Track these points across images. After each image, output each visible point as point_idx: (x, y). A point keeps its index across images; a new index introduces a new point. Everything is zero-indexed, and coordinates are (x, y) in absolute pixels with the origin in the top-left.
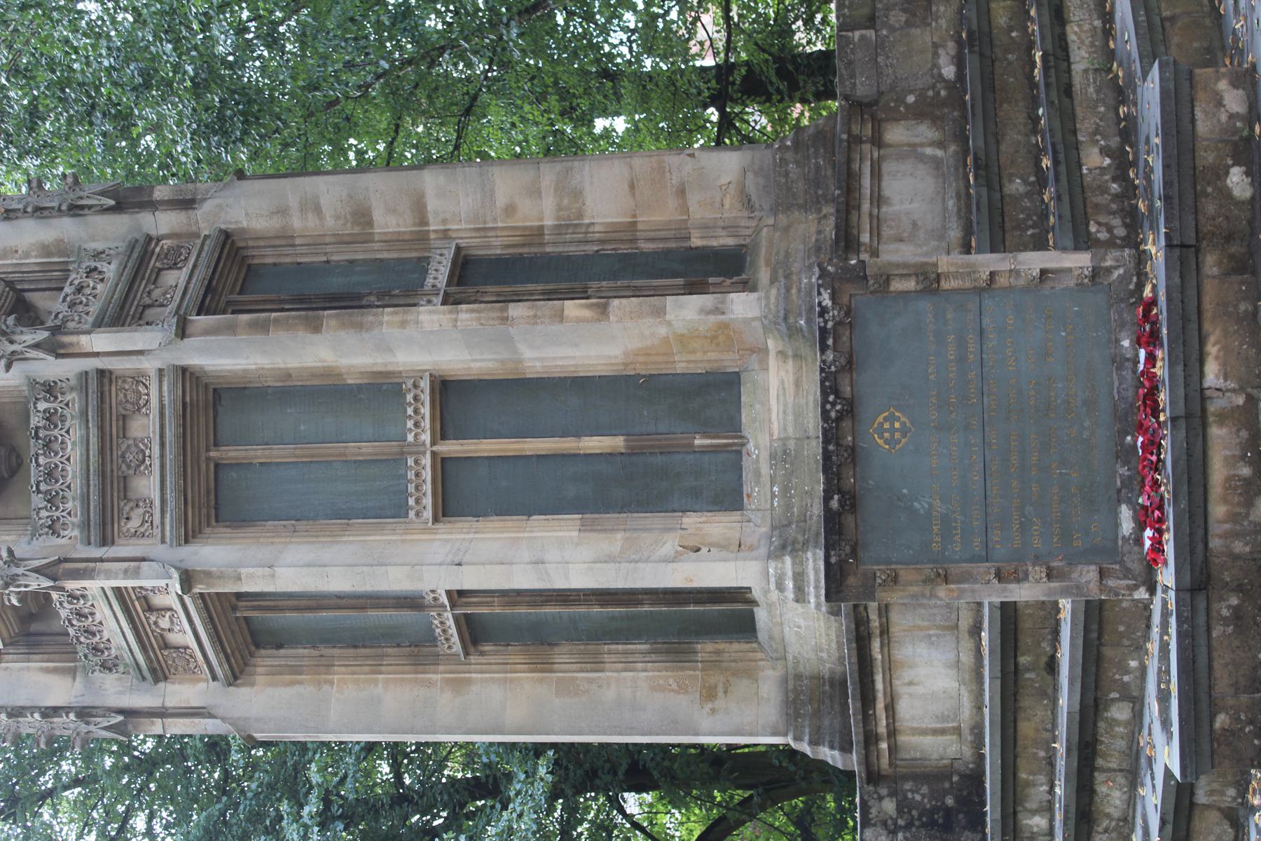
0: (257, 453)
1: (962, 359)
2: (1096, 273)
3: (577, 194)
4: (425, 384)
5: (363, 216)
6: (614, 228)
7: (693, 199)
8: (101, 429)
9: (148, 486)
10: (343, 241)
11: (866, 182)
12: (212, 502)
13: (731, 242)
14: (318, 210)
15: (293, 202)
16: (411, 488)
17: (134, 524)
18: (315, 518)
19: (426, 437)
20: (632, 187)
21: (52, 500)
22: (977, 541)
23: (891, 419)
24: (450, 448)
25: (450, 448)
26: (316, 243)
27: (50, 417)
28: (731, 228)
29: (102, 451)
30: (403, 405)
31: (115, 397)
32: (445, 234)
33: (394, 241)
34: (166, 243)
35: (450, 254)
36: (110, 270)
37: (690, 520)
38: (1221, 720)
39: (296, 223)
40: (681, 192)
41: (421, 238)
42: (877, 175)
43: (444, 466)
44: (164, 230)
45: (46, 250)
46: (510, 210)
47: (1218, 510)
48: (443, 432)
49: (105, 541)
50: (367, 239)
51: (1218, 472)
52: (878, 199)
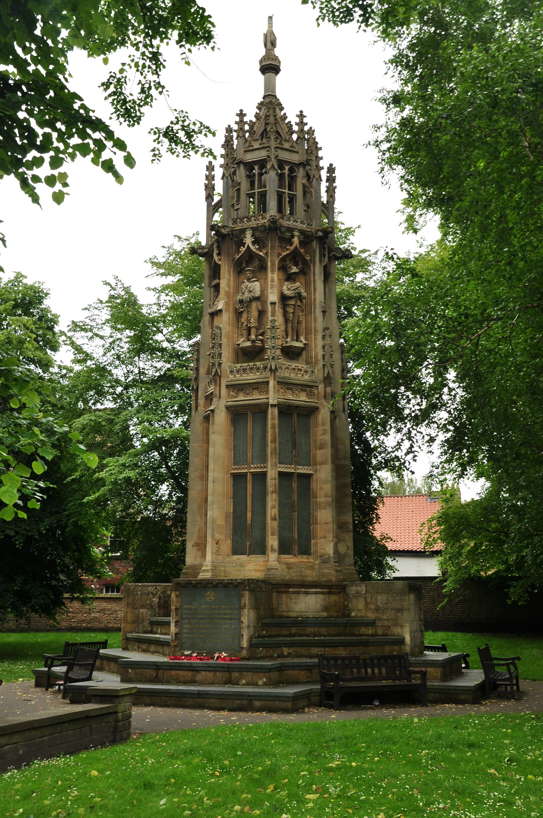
0: (250, 425)
1: (225, 614)
2: (242, 648)
3: (324, 508)
4: (265, 470)
5: (322, 447)
6: (316, 518)
7: (323, 540)
8: (255, 383)
9: (241, 397)
10: (315, 441)
11: (314, 590)
12: (237, 414)
13: (312, 551)
14: (323, 434)
15: (325, 428)
16: (240, 466)
17: (232, 393)
18: (234, 441)
19: (252, 470)
20: (326, 523)
21: (238, 371)
22: (185, 616)
23: (213, 596)
24: (249, 477)
25: (249, 477)
26: (315, 434)
27: (258, 369)
28: (316, 552)
29: (248, 384)
30: (260, 464)
31: (263, 386)
32: (316, 471)
33: (315, 456)
34: (316, 391)
35: (311, 472)
36: (306, 377)
37: (229, 542)
38: (130, 671)
39: (320, 428)
40: (325, 537)
41: (315, 464)
42: (316, 593)
43: (245, 475)
44: (320, 390)
45: (316, 357)
46: (322, 489)
47: (173, 673)
48: (253, 474)
49: (227, 386)
50: (316, 449)
51: (181, 673)
52: (307, 593)
